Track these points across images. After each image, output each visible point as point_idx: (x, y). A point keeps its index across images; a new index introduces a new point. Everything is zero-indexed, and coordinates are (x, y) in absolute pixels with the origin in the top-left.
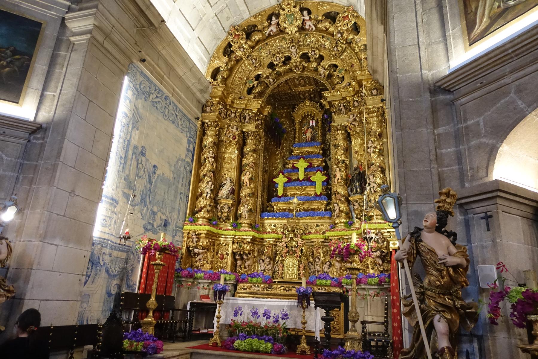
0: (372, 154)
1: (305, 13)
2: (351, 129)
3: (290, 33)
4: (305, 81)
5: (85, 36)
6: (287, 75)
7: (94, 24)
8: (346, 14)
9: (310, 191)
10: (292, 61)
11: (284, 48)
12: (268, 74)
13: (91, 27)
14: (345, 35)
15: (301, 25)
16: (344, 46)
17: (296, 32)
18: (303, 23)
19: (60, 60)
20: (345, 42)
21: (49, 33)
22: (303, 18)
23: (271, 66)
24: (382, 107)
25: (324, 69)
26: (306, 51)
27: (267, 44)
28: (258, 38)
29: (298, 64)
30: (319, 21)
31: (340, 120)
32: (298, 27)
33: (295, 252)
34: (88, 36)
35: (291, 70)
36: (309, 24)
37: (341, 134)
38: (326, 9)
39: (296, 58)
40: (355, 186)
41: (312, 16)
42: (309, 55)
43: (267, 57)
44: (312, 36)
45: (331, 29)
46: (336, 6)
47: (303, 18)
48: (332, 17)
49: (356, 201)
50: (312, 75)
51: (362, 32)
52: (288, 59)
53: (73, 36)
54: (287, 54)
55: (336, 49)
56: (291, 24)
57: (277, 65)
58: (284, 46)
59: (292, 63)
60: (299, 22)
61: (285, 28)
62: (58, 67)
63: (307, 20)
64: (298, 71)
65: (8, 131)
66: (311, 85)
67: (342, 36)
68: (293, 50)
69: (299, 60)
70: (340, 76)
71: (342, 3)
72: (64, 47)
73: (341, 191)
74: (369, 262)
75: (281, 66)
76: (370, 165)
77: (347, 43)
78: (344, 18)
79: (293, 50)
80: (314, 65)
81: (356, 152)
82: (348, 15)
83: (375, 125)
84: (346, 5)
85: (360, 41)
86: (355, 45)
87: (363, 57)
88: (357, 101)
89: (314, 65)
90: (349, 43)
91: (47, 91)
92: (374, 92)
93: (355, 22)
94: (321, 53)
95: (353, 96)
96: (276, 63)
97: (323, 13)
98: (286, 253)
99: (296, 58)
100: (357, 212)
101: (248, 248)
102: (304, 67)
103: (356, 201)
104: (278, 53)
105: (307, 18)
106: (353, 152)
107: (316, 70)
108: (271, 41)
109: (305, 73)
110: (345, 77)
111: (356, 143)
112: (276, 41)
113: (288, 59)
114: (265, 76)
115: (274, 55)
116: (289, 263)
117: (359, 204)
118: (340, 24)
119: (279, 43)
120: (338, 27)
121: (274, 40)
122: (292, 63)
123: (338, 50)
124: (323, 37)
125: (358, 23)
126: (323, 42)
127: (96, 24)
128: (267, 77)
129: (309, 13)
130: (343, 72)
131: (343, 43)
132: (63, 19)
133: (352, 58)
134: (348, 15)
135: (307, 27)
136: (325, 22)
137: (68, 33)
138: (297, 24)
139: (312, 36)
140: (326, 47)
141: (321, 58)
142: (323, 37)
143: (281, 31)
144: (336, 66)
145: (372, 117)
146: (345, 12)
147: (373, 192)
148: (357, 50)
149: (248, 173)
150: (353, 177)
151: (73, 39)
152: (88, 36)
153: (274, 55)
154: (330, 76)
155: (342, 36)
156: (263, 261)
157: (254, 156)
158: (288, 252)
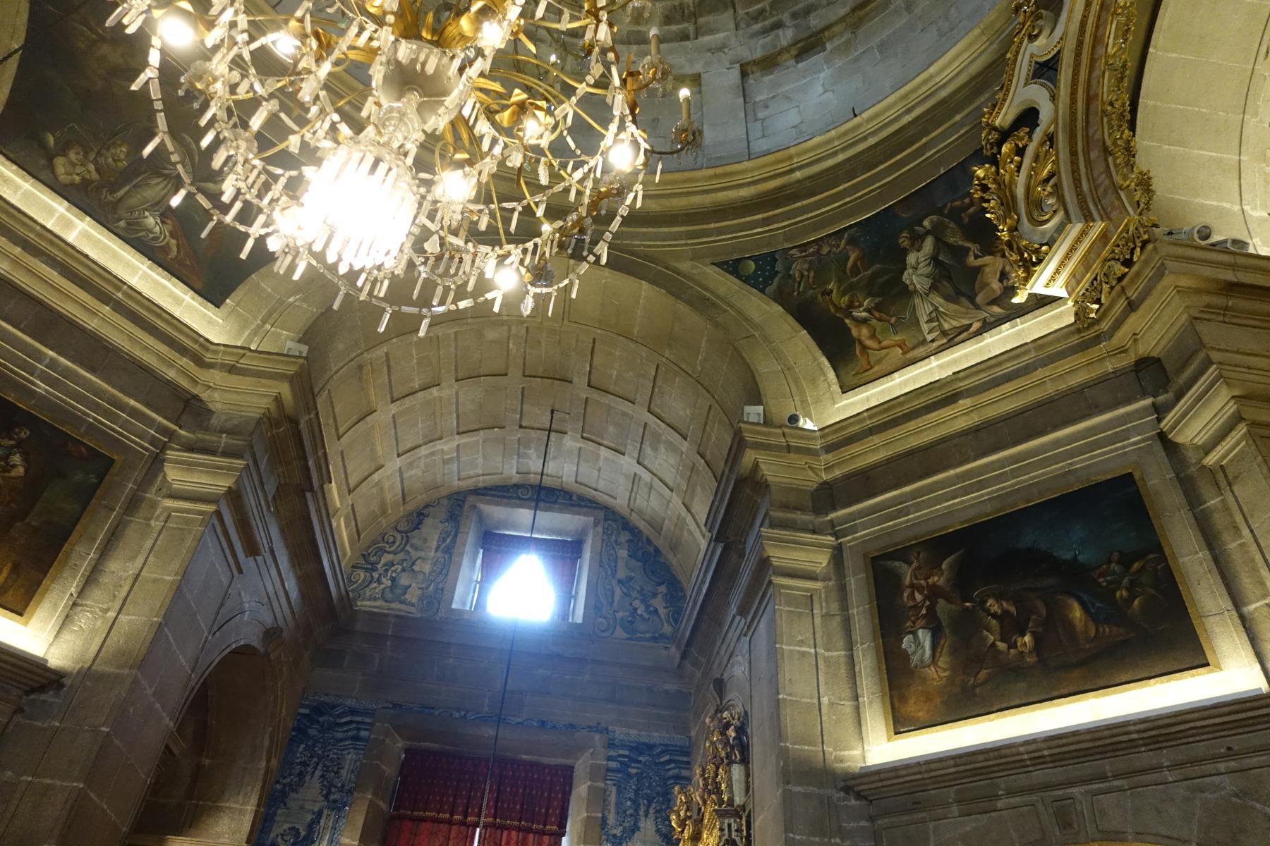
5: (1234, 433)
7: (1233, 397)
13: (1232, 408)
19: (1219, 520)
21: (1157, 481)
34: (1242, 429)
53: (1207, 454)
62: (1226, 536)
65: (1236, 742)
72: (1205, 489)
91: (1246, 604)
127: (1236, 393)
132: (1162, 436)
137: (1192, 457)
151: (1211, 460)
152: (1242, 429)
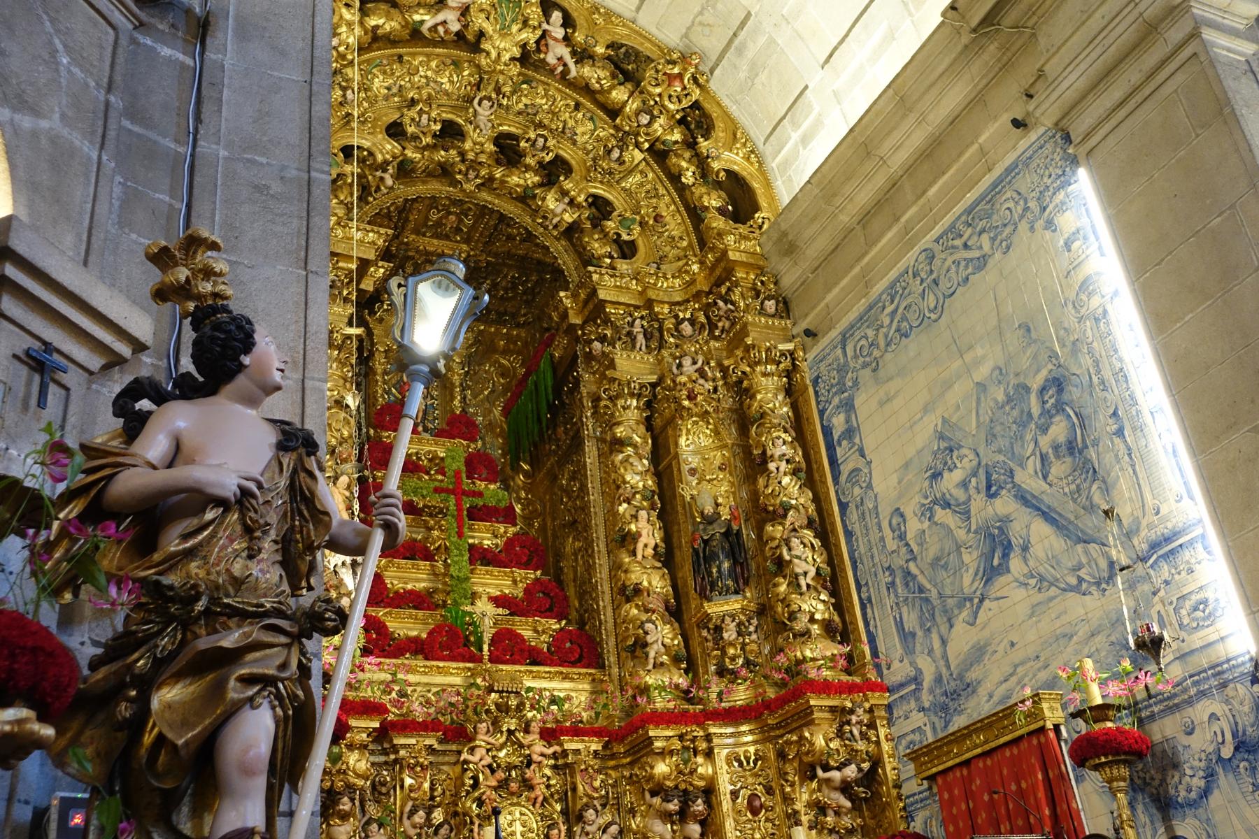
0: (786, 480)
1: (557, 16)
2: (691, 397)
3: (494, 54)
4: (461, 221)
6: (424, 183)
8: (676, 71)
9: (484, 585)
10: (468, 145)
11: (447, 93)
12: (388, 157)
14: (658, 127)
15: (532, 45)
16: (639, 156)
17: (513, 59)
18: (538, 42)
20: (646, 145)
22: (545, 26)
23: (395, 131)
24: (792, 353)
25: (572, 203)
26: (513, 130)
27: (400, 57)
28: (387, 27)
29: (483, 158)
30: (583, 55)
31: (633, 365)
32: (524, 46)
33: (528, 785)
35: (445, 172)
36: (557, 52)
37: (637, 408)
38: (621, 34)
39: (479, 140)
40: (719, 568)
41: (579, 37)
42: (523, 144)
43: (386, 98)
44: (541, 90)
45: (619, 94)
46: (641, 35)
47: (545, 26)
48: (627, 64)
49: (733, 617)
50: (510, 209)
51: (720, 133)
52: (451, 132)
54: (450, 116)
55: (616, 154)
56: (504, 32)
57: (415, 138)
58: (447, 86)
59: (462, 154)
60: (530, 36)
61: (481, 34)
63: (555, 39)
64: (468, 180)
66: (467, 241)
67: (649, 124)
68: (484, 111)
69: (490, 147)
70: (625, 237)
71: (661, 36)
73: (656, 582)
74: (799, 806)
75: (427, 147)
76: (764, 513)
77: (652, 146)
78: (671, 78)
79: (484, 111)
80: (532, 179)
81: (693, 472)
82: (680, 76)
83: (780, 397)
84: (672, 44)
85: (718, 158)
86: (684, 164)
87: (714, 203)
88: (692, 321)
89: (532, 179)
90: (659, 154)
92: (770, 305)
93: (696, 105)
94: (561, 152)
95: (678, 303)
96: (411, 130)
97: (609, 39)
98: (495, 789)
99: (479, 140)
100: (731, 651)
101: (363, 766)
102: (491, 179)
103: (733, 617)
104: (429, 101)
105: (559, 33)
106: (685, 468)
107: (525, 198)
108: (413, 55)
109: (484, 195)
110: (640, 243)
111: (695, 444)
112: (429, 61)
113: (451, 132)
114: (380, 158)
115: (413, 102)
116: (510, 825)
117: (738, 625)
118: (658, 90)
119: (437, 72)
120: (650, 95)
121: (427, 55)
122: (462, 154)
123: (620, 161)
124: (577, 107)
125: (706, 105)
126: (571, 123)
128: (384, 166)
129: (568, 22)
130: (637, 229)
131: (637, 145)
133: (657, 196)
134: (680, 76)
135: (551, 59)
136: (604, 68)
138: (524, 35)
139: (541, 90)
140: (578, 138)
141: (554, 171)
142: (577, 107)
143: (468, 42)
144: (601, 207)
145: (764, 375)
146: (674, 63)
147: (804, 588)
148: (688, 178)
149: (344, 480)
150: (706, 542)
153: (413, 102)
154: (571, 232)
155: (649, 124)
156: (381, 825)
157: (349, 423)
158: (503, 785)
